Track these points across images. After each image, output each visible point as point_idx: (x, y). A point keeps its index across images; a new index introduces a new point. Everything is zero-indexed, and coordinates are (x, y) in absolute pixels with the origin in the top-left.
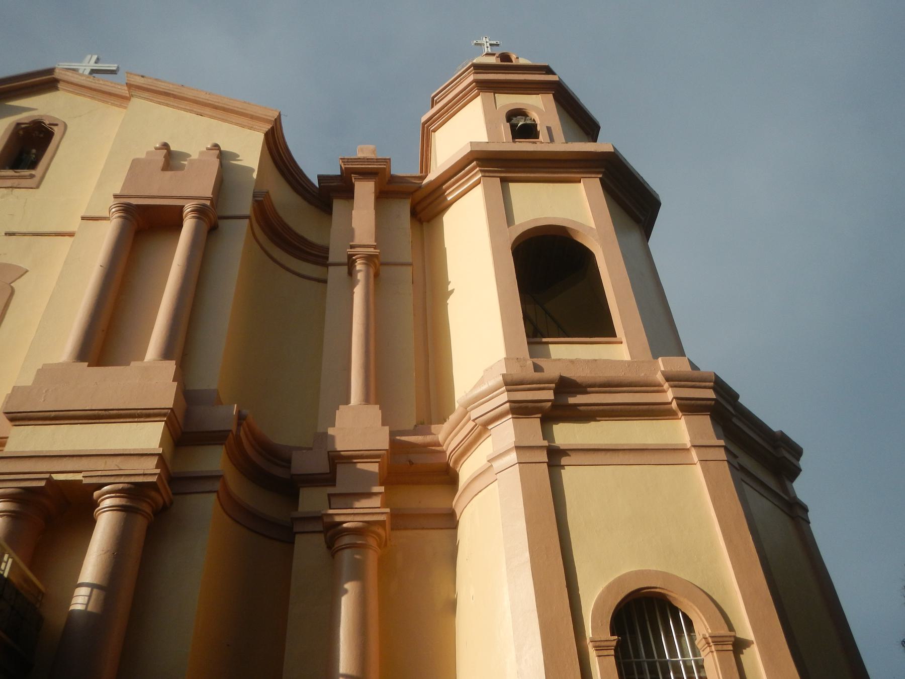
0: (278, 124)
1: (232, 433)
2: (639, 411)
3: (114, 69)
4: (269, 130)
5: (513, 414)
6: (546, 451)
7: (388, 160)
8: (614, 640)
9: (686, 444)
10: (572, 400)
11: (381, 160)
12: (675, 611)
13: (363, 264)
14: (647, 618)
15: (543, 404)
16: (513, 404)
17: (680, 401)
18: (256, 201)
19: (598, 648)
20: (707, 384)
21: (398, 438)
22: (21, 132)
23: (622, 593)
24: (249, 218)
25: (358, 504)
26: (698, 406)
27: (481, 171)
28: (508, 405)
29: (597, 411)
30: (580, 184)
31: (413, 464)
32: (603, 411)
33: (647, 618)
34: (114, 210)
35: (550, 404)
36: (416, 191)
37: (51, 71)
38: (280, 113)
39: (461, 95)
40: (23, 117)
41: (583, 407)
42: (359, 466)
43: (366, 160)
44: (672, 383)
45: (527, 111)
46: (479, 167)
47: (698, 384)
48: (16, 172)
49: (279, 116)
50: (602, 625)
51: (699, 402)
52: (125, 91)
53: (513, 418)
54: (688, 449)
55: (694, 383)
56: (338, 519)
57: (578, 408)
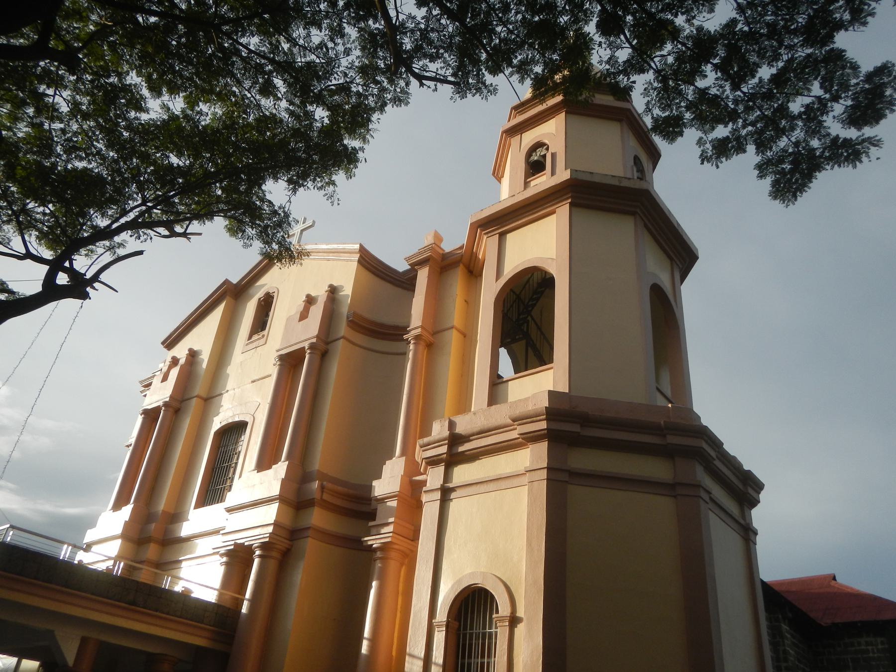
3: (311, 224)
10: (461, 449)
18: (350, 321)
20: (538, 418)
21: (414, 478)
22: (263, 303)
25: (383, 531)
27: (485, 234)
29: (478, 453)
32: (480, 452)
34: (277, 359)
40: (260, 294)
42: (389, 504)
46: (482, 231)
47: (535, 419)
51: (536, 433)
56: (370, 543)
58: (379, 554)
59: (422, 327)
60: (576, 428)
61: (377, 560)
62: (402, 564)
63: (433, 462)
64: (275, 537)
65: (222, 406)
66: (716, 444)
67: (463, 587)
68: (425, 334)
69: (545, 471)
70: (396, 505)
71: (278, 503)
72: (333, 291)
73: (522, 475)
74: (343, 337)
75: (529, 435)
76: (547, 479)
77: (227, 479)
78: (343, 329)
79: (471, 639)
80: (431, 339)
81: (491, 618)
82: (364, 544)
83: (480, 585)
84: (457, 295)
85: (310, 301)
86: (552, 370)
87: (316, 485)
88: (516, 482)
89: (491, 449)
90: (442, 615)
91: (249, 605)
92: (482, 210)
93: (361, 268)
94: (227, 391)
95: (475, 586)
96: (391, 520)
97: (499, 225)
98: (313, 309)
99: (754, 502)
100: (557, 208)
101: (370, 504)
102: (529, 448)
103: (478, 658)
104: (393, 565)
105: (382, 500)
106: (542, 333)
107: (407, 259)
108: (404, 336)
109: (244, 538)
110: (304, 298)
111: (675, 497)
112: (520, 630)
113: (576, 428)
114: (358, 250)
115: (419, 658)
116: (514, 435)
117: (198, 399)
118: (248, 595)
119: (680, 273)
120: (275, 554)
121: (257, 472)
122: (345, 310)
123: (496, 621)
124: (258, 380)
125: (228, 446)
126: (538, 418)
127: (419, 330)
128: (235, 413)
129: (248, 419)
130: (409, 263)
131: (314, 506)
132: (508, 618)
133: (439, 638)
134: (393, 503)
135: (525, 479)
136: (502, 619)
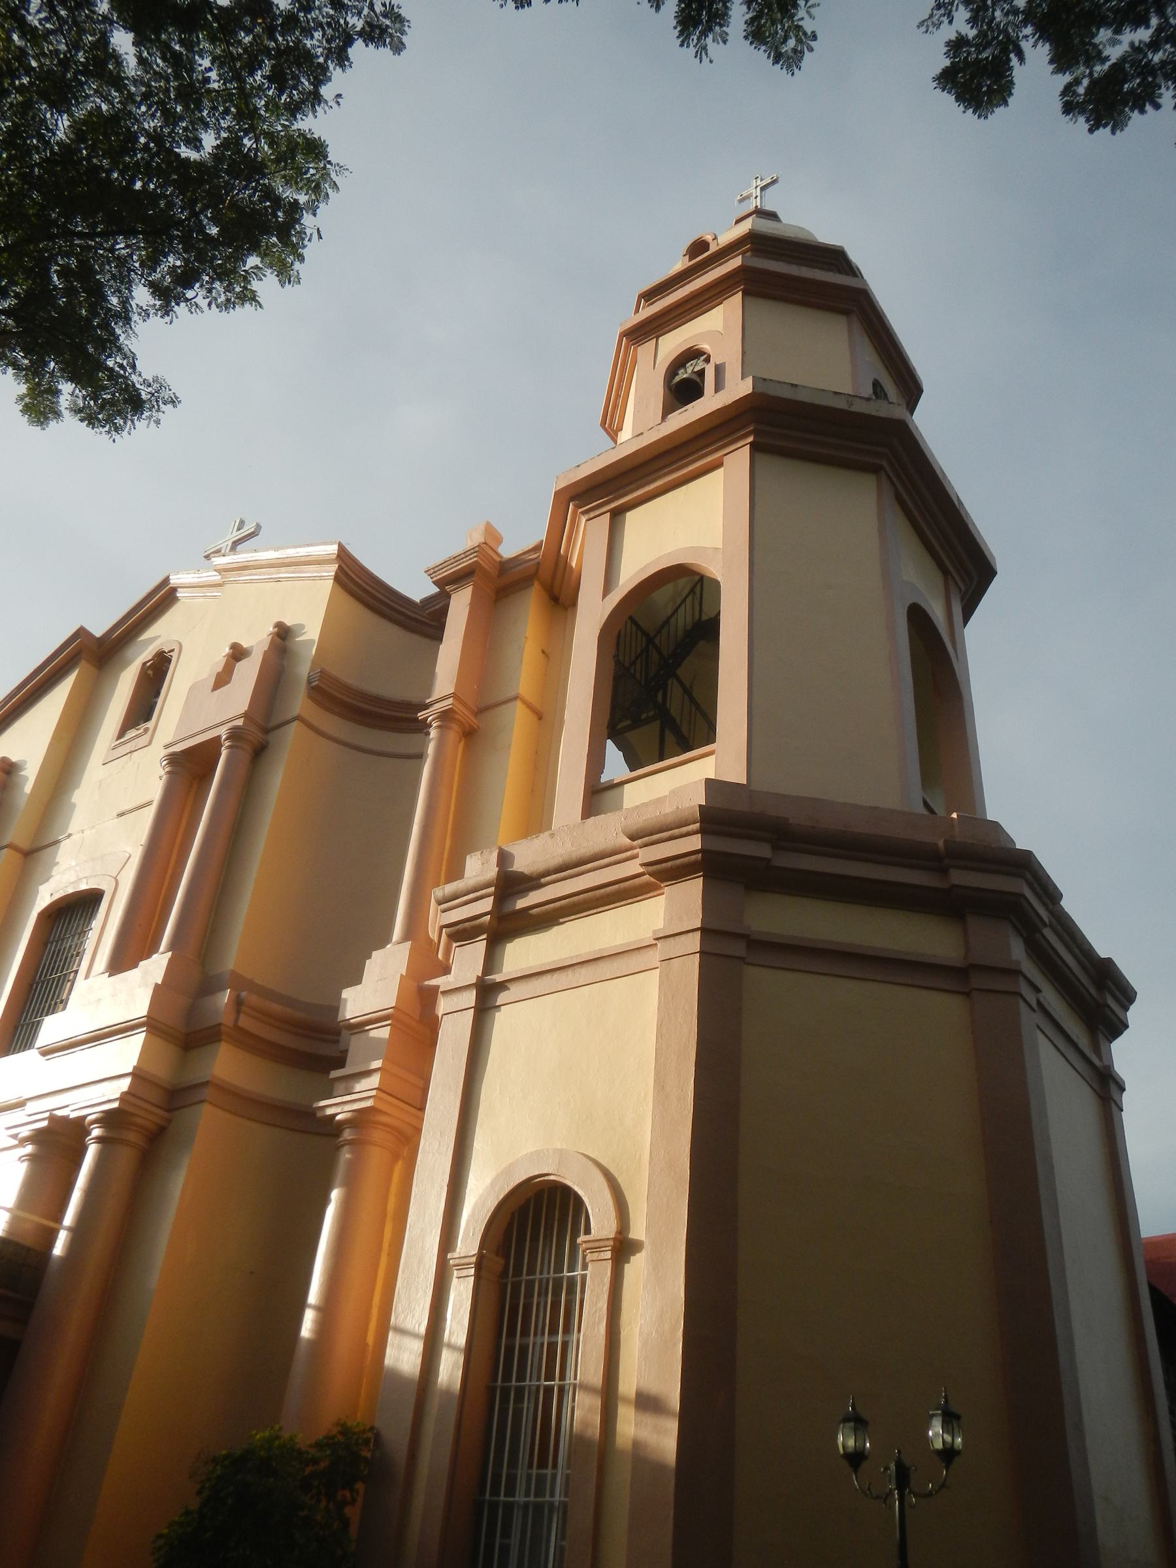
1: (225, 1025)
2: (608, 895)
3: (252, 530)
7: (477, 549)
10: (521, 903)
11: (469, 553)
18: (313, 688)
22: (150, 672)
24: (297, 719)
27: (583, 513)
29: (555, 910)
32: (561, 908)
33: (557, 1217)
34: (165, 762)
36: (537, 569)
37: (166, 581)
42: (373, 1034)
43: (453, 561)
46: (577, 507)
47: (676, 832)
48: (137, 730)
56: (329, 1112)
58: (347, 1134)
59: (454, 695)
60: (762, 851)
61: (343, 1146)
62: (396, 1157)
63: (462, 933)
64: (132, 1099)
65: (58, 863)
66: (1050, 894)
67: (516, 1184)
68: (460, 708)
69: (698, 934)
70: (387, 1036)
71: (144, 1034)
72: (283, 634)
73: (649, 949)
74: (298, 718)
75: (664, 865)
76: (702, 952)
77: (56, 1003)
78: (299, 703)
79: (529, 1295)
80: (474, 721)
81: (574, 1247)
82: (319, 1114)
83: (552, 1178)
84: (526, 638)
85: (238, 653)
86: (714, 756)
87: (226, 996)
88: (634, 962)
89: (585, 901)
90: (468, 1243)
91: (69, 1239)
92: (578, 466)
93: (339, 590)
94: (70, 835)
95: (542, 1179)
96: (377, 1064)
98: (240, 666)
99: (1117, 1028)
100: (725, 455)
101: (337, 1042)
102: (663, 894)
103: (543, 1334)
104: (376, 1157)
105: (360, 1027)
106: (693, 701)
107: (430, 572)
108: (419, 714)
109: (74, 1106)
110: (227, 650)
111: (967, 994)
112: (637, 1268)
113: (762, 851)
114: (336, 555)
115: (415, 1336)
116: (633, 867)
117: (9, 850)
118: (69, 1219)
119: (962, 600)
120: (132, 1136)
121: (109, 976)
122: (304, 669)
123: (584, 1251)
124: (131, 811)
125: (63, 940)
126: (684, 830)
127: (450, 701)
128: (81, 875)
129: (105, 885)
130: (435, 579)
131: (220, 1040)
132: (611, 1243)
133: (461, 1293)
134: (382, 1033)
135: (653, 957)
136: (597, 1247)
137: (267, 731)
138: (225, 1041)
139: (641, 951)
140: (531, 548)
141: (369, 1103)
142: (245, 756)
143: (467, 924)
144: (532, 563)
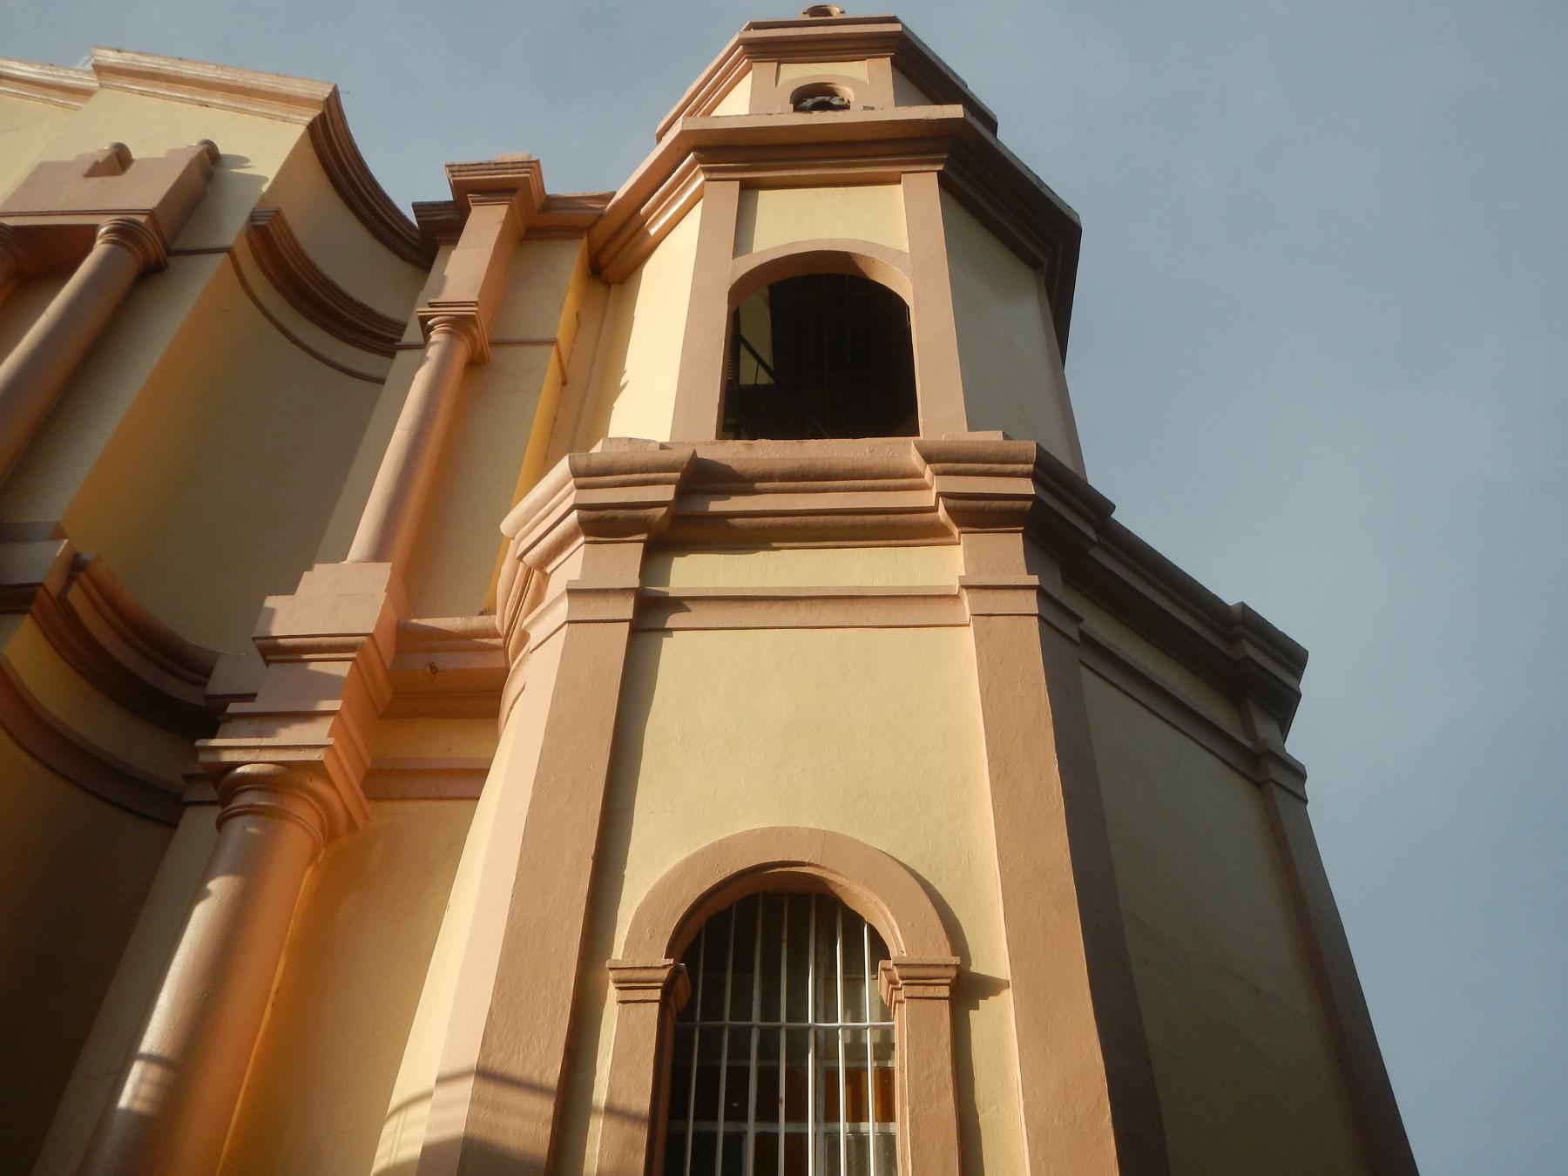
0: (334, 109)
1: (47, 591)
2: (864, 526)
4: (315, 119)
5: (587, 534)
6: (632, 601)
7: (533, 164)
8: (665, 967)
9: (953, 587)
10: (716, 506)
11: (520, 165)
12: (854, 922)
13: (443, 332)
14: (785, 937)
15: (650, 512)
16: (586, 513)
17: (952, 502)
18: (257, 228)
19: (623, 985)
20: (1019, 467)
21: (415, 621)
23: (719, 872)
24: (228, 252)
26: (992, 512)
27: (704, 170)
28: (575, 514)
30: (899, 186)
31: (437, 670)
32: (784, 527)
33: (785, 937)
35: (663, 510)
38: (335, 90)
39: (719, 73)
41: (739, 520)
42: (313, 666)
43: (493, 167)
44: (938, 466)
45: (839, 87)
46: (698, 160)
47: (997, 467)
49: (335, 90)
50: (650, 938)
52: (90, 82)
53: (586, 542)
54: (956, 597)
55: (988, 466)
56: (227, 757)
57: (730, 521)
67: (735, 871)
75: (973, 503)
89: (824, 527)
96: (325, 705)
97: (751, 161)
101: (204, 685)
137: (171, 253)
138: (34, 617)
139: (929, 600)
140: (596, 194)
141: (315, 756)
142: (130, 264)
143: (621, 513)
144: (590, 212)
